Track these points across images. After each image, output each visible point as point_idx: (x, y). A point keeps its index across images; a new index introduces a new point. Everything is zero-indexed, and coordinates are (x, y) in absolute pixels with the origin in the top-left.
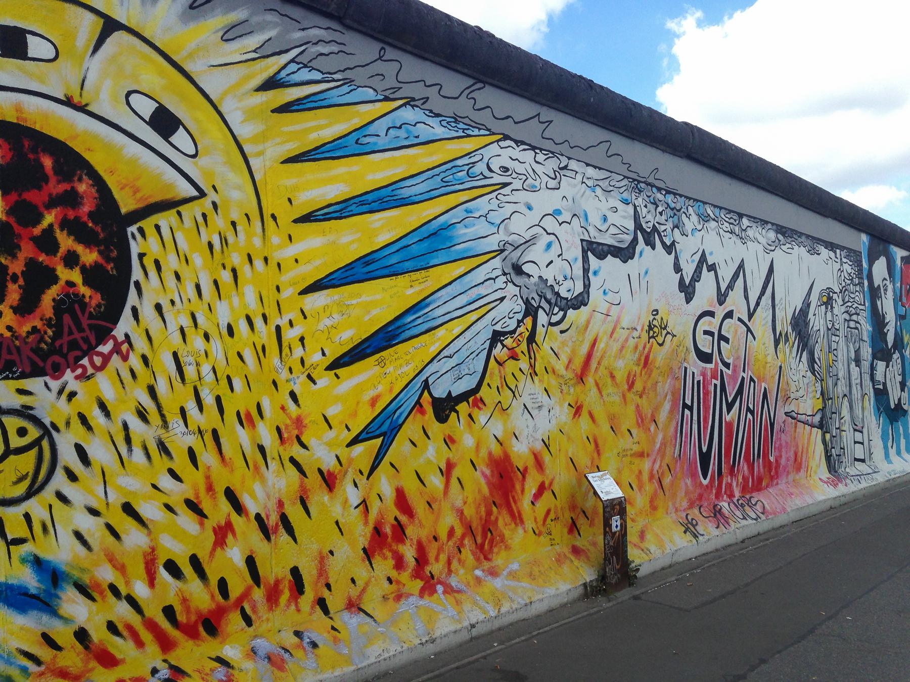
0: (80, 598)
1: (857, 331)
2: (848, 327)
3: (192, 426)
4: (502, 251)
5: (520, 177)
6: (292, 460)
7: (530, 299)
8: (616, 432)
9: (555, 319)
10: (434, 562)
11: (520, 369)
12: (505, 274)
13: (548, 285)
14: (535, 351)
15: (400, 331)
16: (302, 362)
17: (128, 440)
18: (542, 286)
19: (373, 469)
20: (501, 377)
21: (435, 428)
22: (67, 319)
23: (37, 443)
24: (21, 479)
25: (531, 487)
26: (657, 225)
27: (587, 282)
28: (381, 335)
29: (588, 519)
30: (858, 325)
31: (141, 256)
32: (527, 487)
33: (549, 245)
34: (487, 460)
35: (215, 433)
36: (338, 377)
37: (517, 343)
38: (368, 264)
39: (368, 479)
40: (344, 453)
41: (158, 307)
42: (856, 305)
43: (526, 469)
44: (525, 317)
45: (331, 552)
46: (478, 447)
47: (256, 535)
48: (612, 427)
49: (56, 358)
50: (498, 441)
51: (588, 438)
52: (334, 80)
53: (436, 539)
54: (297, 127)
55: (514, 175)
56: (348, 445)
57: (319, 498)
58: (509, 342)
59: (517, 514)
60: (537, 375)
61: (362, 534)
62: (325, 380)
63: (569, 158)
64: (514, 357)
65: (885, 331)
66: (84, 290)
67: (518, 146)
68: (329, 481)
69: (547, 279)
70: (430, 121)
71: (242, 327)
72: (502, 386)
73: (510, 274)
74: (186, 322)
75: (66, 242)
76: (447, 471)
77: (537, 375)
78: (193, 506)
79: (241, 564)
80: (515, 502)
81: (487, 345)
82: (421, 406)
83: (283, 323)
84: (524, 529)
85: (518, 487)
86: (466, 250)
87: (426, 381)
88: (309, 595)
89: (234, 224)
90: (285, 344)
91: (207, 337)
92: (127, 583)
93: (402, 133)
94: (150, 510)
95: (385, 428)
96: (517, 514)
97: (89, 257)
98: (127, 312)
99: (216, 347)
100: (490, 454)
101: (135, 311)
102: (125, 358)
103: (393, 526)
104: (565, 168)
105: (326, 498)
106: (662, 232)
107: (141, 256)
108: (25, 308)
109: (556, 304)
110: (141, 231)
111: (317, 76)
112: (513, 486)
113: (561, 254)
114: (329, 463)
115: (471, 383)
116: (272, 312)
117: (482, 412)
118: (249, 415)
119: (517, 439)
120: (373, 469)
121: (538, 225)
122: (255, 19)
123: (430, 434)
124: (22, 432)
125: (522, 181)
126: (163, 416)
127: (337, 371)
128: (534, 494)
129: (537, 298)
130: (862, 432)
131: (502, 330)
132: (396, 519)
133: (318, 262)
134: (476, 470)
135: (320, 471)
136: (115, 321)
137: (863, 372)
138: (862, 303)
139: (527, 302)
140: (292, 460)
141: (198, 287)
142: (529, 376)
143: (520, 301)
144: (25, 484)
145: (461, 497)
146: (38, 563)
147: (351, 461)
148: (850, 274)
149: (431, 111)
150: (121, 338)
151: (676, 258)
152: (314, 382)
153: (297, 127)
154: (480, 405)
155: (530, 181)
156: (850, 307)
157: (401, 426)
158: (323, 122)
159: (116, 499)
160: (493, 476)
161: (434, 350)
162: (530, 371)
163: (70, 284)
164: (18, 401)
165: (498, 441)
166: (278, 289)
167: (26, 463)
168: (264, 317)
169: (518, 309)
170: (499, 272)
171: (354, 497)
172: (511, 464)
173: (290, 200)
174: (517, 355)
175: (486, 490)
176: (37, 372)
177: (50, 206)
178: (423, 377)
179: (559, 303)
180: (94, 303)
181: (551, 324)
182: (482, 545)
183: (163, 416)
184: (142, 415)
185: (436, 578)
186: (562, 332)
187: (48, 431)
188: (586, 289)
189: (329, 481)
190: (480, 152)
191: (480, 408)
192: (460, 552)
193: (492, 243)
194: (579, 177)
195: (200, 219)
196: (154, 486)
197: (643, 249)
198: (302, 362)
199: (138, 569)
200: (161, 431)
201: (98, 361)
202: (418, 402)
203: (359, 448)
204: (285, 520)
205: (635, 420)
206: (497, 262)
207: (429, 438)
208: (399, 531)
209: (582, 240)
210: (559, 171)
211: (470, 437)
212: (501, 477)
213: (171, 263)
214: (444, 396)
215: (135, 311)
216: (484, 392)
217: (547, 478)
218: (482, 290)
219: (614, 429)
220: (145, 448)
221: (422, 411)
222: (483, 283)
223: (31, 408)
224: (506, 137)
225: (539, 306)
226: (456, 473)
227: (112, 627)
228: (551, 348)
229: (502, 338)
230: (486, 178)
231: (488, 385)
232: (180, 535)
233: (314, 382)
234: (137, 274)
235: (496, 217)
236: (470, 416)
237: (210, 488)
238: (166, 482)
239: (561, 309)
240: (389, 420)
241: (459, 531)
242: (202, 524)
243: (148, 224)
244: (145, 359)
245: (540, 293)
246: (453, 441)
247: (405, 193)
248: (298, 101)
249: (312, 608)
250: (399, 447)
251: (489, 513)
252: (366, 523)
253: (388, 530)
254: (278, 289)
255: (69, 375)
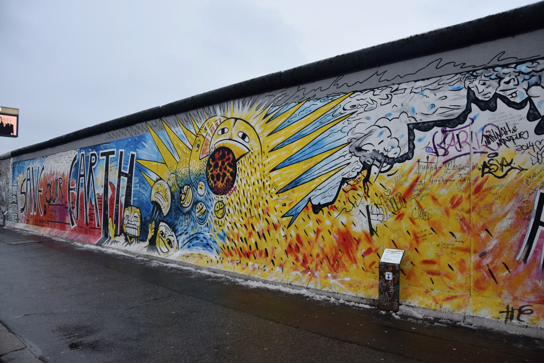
0: (228, 240)
3: (246, 207)
4: (349, 143)
5: (363, 106)
6: (266, 219)
7: (366, 161)
8: (437, 232)
9: (383, 169)
10: (310, 263)
11: (358, 194)
12: (350, 152)
13: (380, 153)
14: (369, 186)
15: (300, 181)
16: (269, 192)
17: (235, 209)
18: (375, 154)
19: (289, 226)
20: (346, 198)
21: (312, 215)
22: (228, 183)
23: (223, 208)
24: (221, 214)
25: (363, 247)
26: (501, 93)
27: (411, 146)
28: (294, 183)
29: (405, 275)
31: (239, 168)
32: (360, 248)
33: (381, 133)
34: (337, 232)
35: (250, 209)
36: (279, 196)
37: (357, 183)
38: (290, 160)
39: (287, 229)
40: (280, 219)
41: (241, 179)
43: (360, 240)
44: (362, 170)
45: (276, 248)
46: (332, 226)
47: (257, 237)
48: (432, 229)
49: (226, 191)
50: (343, 224)
51: (408, 232)
52: (282, 106)
53: (311, 255)
54: (271, 125)
55: (359, 107)
56: (281, 217)
57: (272, 231)
58: (351, 182)
59: (353, 258)
60: (369, 197)
61: (285, 246)
62: (275, 197)
63: (399, 84)
64: (354, 188)
66: (230, 177)
67: (362, 93)
68: (275, 227)
69: (379, 151)
70: (316, 103)
71: (256, 182)
72: (347, 202)
73: (354, 152)
74: (245, 182)
75: (228, 168)
76: (317, 232)
77: (369, 197)
78: (245, 226)
79: (254, 243)
80: (352, 253)
81: (339, 184)
82: (307, 207)
83: (264, 180)
84: (357, 266)
85: (354, 246)
86: (330, 146)
87: (310, 198)
88: (269, 258)
89: (256, 156)
90: (265, 187)
91: (249, 186)
92: (234, 240)
93: (305, 112)
94: (238, 225)
95: (293, 213)
96: (353, 258)
97: (231, 170)
98: (236, 181)
99: (251, 188)
100: (339, 229)
101: (237, 180)
102: (235, 191)
103: (295, 246)
104: (396, 90)
105: (274, 232)
106: (509, 95)
107: (239, 168)
108: (222, 182)
109: (385, 162)
110: (239, 163)
111: (278, 107)
112: (351, 246)
113: (391, 136)
114: (276, 222)
115: (330, 200)
116: (262, 178)
117: (335, 212)
118: (257, 205)
119: (355, 225)
120: (289, 226)
121: (374, 125)
122: (264, 100)
123: (310, 218)
124: (221, 205)
125: (364, 108)
126: (241, 204)
127: (279, 194)
128: (364, 252)
129: (371, 161)
131: (347, 177)
132: (296, 244)
133: (274, 163)
134: (331, 235)
135: (273, 223)
136: (234, 183)
139: (364, 164)
140: (266, 219)
141: (248, 174)
142: (364, 197)
143: (360, 163)
144: (222, 215)
145: (323, 243)
146: (223, 231)
147: (282, 222)
149: (316, 99)
150: (235, 187)
151: (533, 108)
152: (272, 198)
153: (271, 125)
154: (334, 209)
155: (370, 106)
157: (299, 213)
158: (278, 120)
159: (233, 221)
160: (340, 238)
161: (313, 187)
162: (365, 195)
163: (228, 176)
164: (220, 199)
165: (343, 224)
166: (264, 172)
167: (221, 211)
168: (261, 180)
169: (358, 167)
170: (348, 152)
171: (283, 234)
172: (351, 236)
173: (268, 146)
174: (356, 188)
175: (336, 244)
176: (223, 194)
177: (226, 161)
178: (309, 197)
179: (387, 161)
180: (231, 179)
181: (380, 172)
182: (333, 266)
183: (241, 204)
184: (237, 204)
185: (311, 269)
186: (388, 175)
187: (225, 205)
188: (411, 151)
189: (275, 227)
190: (339, 104)
191: (334, 210)
192: (322, 264)
193: (345, 141)
194: (408, 91)
195: (249, 157)
196: (239, 220)
197: (478, 114)
198: (269, 192)
199: (236, 237)
200: (240, 208)
201: (231, 191)
202: (306, 206)
203: (285, 219)
204: (263, 234)
205: (459, 226)
206: (347, 148)
207: (310, 219)
208: (297, 248)
209: (408, 125)
210: (391, 93)
211: (328, 221)
212: (344, 240)
213: (243, 169)
214: (317, 204)
215: (237, 180)
216: (336, 204)
217: (374, 246)
218: (337, 162)
219: (435, 230)
220: (238, 211)
221: (308, 209)
222: (338, 158)
223: (222, 201)
224: (354, 92)
225: (373, 164)
226: (321, 234)
227: (232, 248)
228: (381, 184)
229: (347, 181)
230: (342, 114)
231: (339, 201)
232: (243, 232)
233: (272, 198)
234: (238, 173)
235: (346, 130)
236: (329, 213)
237: (248, 223)
238: (241, 219)
239: (388, 164)
240: (294, 212)
241: (321, 256)
242: (247, 231)
243: (240, 161)
244: (238, 191)
245: (373, 158)
246: (320, 221)
247: (304, 133)
248: (272, 117)
249: (270, 261)
250: (298, 221)
251: (337, 253)
252: (286, 243)
253: (293, 247)
254: (264, 172)
255: (228, 195)
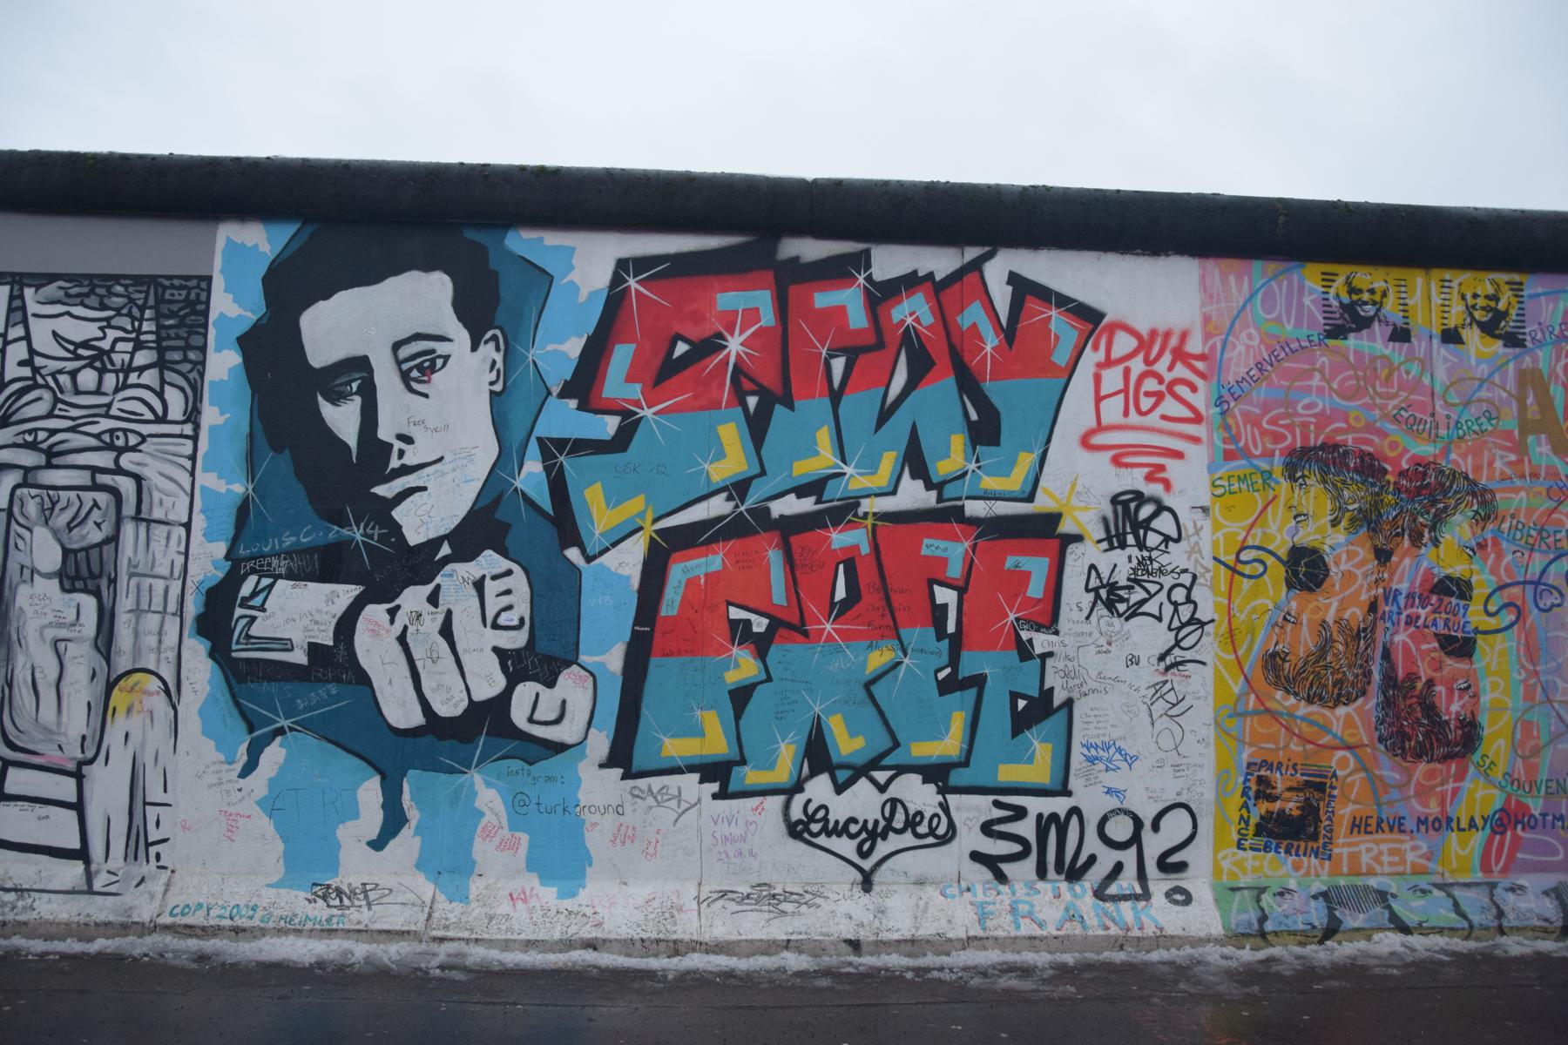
1: (103, 498)
2: (25, 484)
30: (126, 485)
42: (106, 424)
65: (382, 490)
130: (78, 776)
137: (125, 604)
138: (176, 412)
148: (85, 344)
156: (53, 432)
